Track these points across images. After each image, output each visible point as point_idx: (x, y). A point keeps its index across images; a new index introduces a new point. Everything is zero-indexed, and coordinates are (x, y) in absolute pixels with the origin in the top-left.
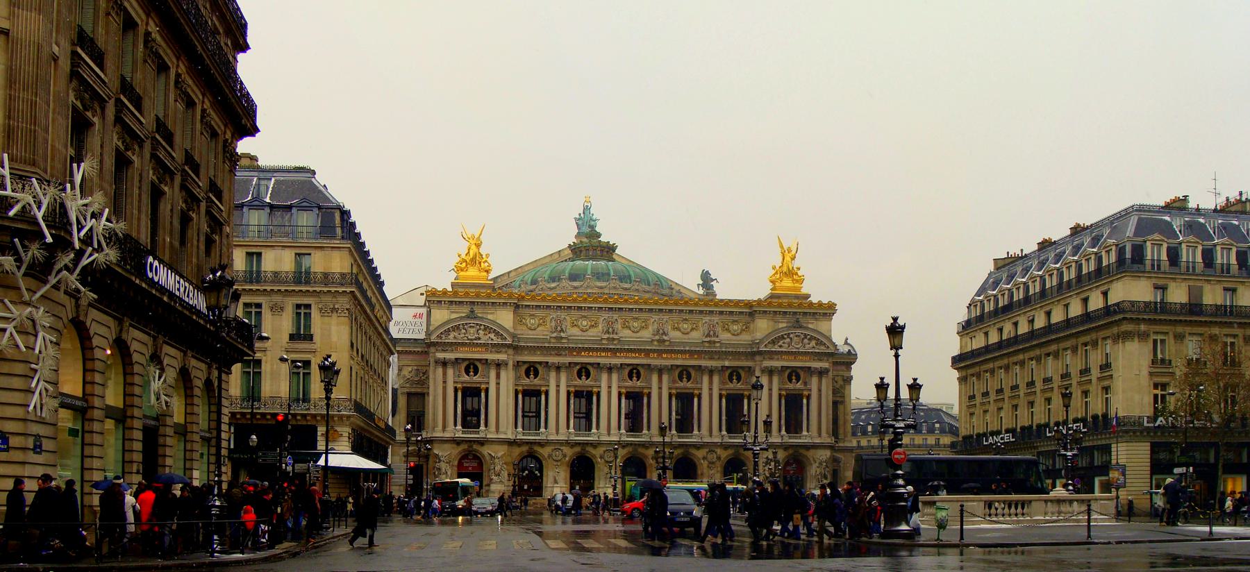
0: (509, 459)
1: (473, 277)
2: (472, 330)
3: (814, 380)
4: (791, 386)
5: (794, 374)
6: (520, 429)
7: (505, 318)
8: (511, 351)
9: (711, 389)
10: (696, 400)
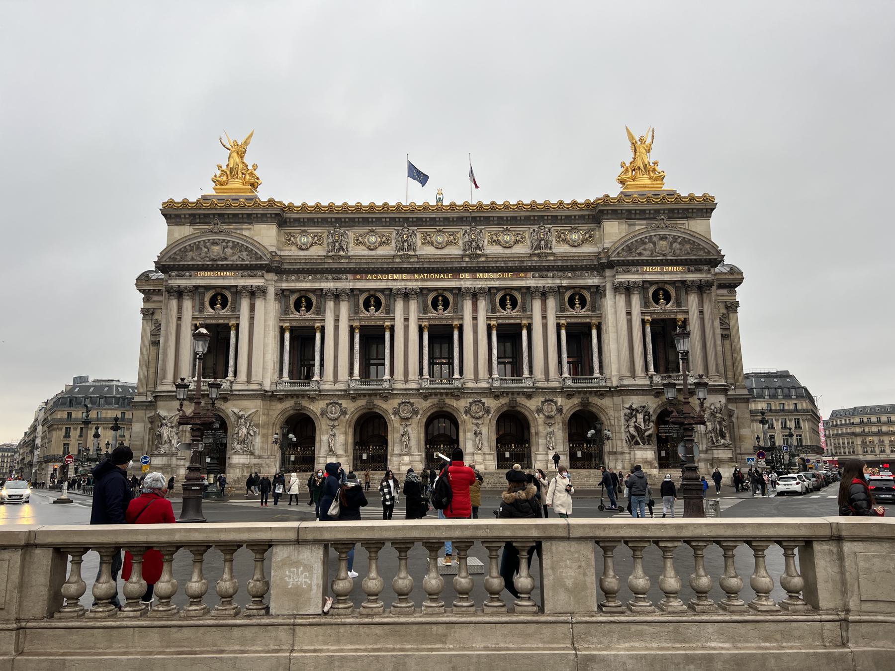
0: (262, 419)
2: (216, 249)
3: (692, 301)
4: (658, 308)
5: (661, 292)
6: (286, 378)
7: (266, 236)
8: (271, 276)
9: (544, 318)
10: (525, 333)
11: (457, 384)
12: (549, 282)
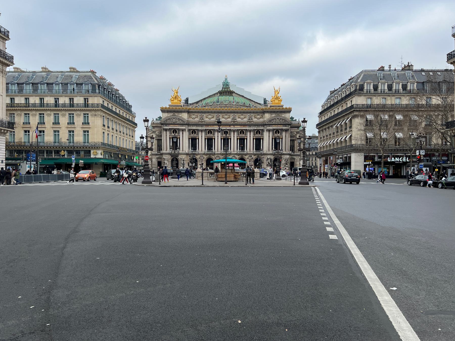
1: (175, 103)
2: (174, 120)
3: (284, 134)
4: (276, 135)
5: (277, 131)
8: (187, 126)
11: (229, 152)
12: (252, 128)
